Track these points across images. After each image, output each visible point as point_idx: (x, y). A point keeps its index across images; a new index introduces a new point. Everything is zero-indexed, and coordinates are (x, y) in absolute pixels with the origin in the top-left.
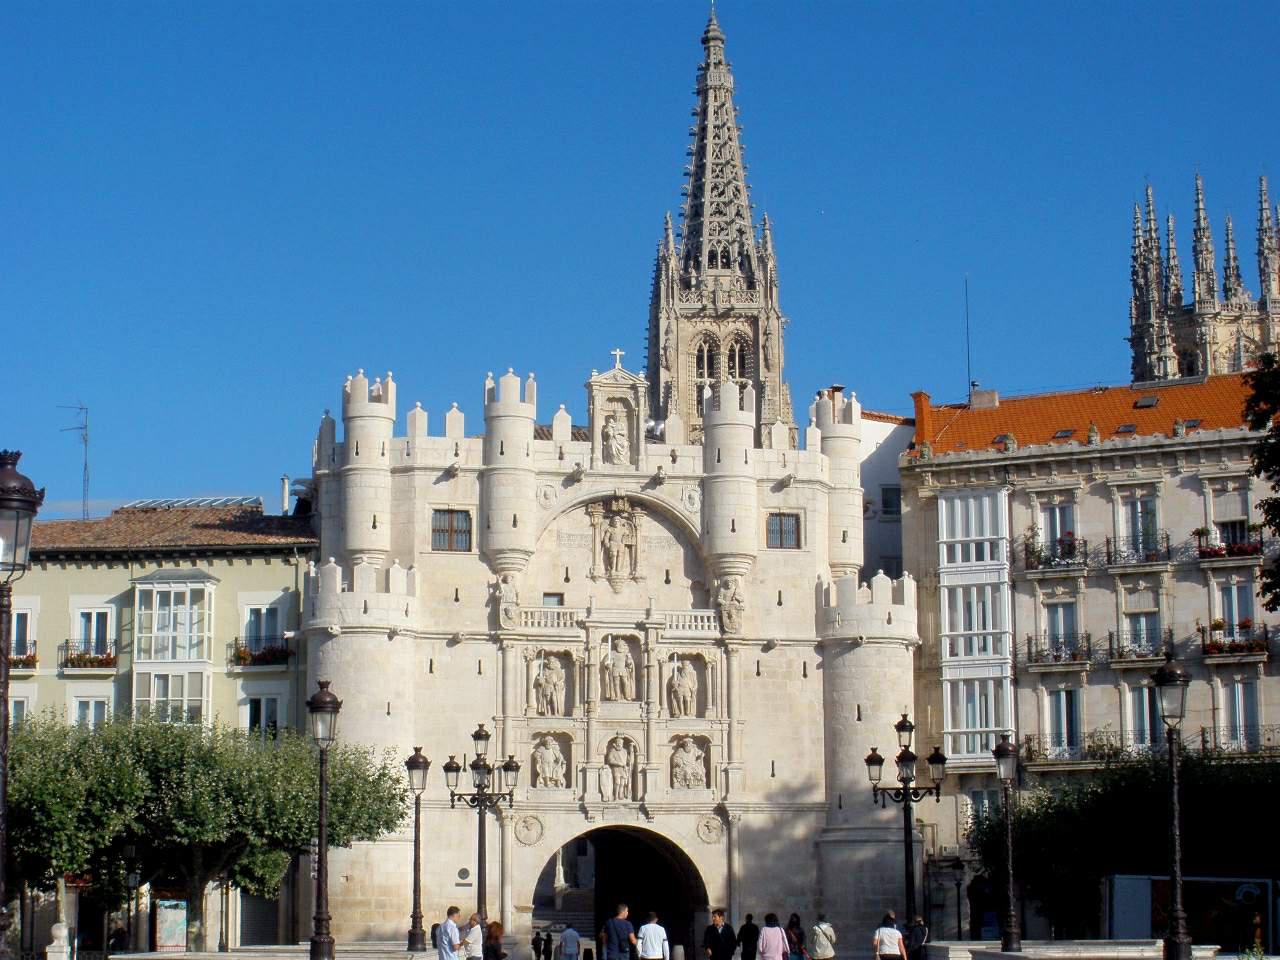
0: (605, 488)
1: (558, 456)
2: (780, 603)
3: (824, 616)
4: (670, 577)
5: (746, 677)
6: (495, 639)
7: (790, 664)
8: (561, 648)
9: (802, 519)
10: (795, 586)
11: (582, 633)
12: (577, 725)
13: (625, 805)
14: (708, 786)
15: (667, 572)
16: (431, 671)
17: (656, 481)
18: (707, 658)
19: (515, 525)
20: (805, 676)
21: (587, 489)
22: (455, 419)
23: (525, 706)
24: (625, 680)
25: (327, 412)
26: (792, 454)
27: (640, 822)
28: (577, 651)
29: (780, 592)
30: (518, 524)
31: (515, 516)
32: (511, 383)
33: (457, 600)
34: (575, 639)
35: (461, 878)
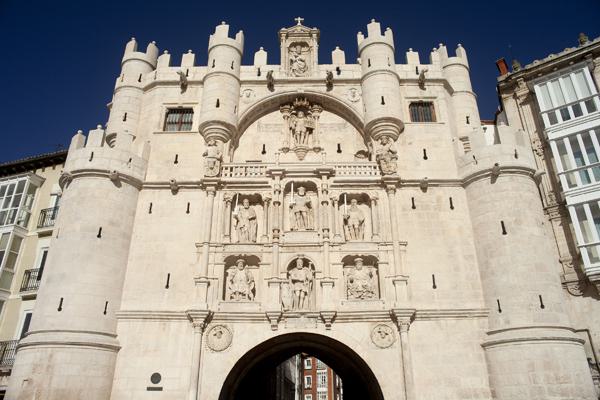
1: (257, 74)
2: (425, 158)
3: (461, 164)
5: (404, 209)
6: (202, 186)
7: (439, 199)
8: (252, 192)
10: (436, 146)
12: (266, 249)
13: (303, 314)
15: (339, 145)
16: (150, 212)
17: (330, 83)
19: (218, 106)
20: (452, 208)
21: (279, 89)
22: (188, 58)
24: (304, 214)
26: (422, 67)
27: (320, 329)
28: (265, 194)
32: (223, 29)
33: (176, 162)
35: (154, 382)
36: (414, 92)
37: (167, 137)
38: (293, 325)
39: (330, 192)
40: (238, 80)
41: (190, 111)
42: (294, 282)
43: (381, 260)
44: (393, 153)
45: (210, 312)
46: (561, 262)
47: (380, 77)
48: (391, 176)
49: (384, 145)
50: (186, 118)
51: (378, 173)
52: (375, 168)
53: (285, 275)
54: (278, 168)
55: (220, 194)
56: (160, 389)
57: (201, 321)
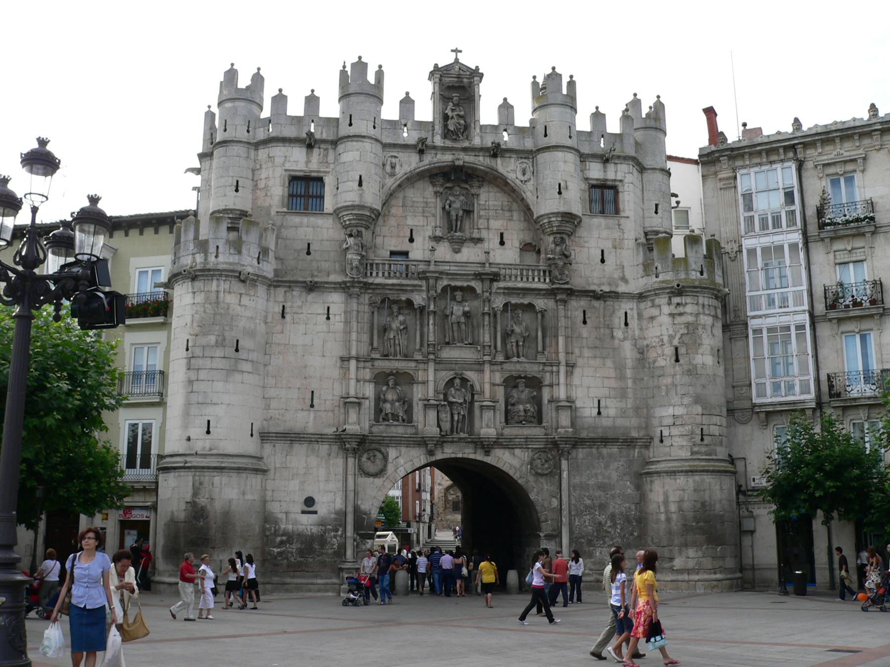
0: (447, 158)
2: (603, 261)
4: (505, 240)
6: (343, 287)
8: (403, 298)
9: (620, 189)
11: (424, 283)
13: (460, 439)
14: (540, 422)
15: (502, 235)
18: (537, 308)
19: (360, 184)
21: (429, 159)
23: (370, 348)
24: (463, 327)
25: (209, 107)
27: (479, 456)
29: (602, 251)
30: (364, 183)
31: (360, 177)
33: (309, 253)
34: (416, 289)
36: (595, 171)
37: (296, 219)
38: (450, 451)
39: (492, 299)
40: (381, 143)
41: (320, 180)
42: (452, 403)
43: (547, 381)
44: (566, 257)
45: (364, 435)
46: (733, 387)
47: (559, 155)
48: (563, 286)
49: (557, 245)
50: (313, 189)
51: (548, 280)
52: (544, 272)
53: (442, 397)
54: (432, 268)
55: (366, 298)
56: (315, 512)
57: (354, 445)
